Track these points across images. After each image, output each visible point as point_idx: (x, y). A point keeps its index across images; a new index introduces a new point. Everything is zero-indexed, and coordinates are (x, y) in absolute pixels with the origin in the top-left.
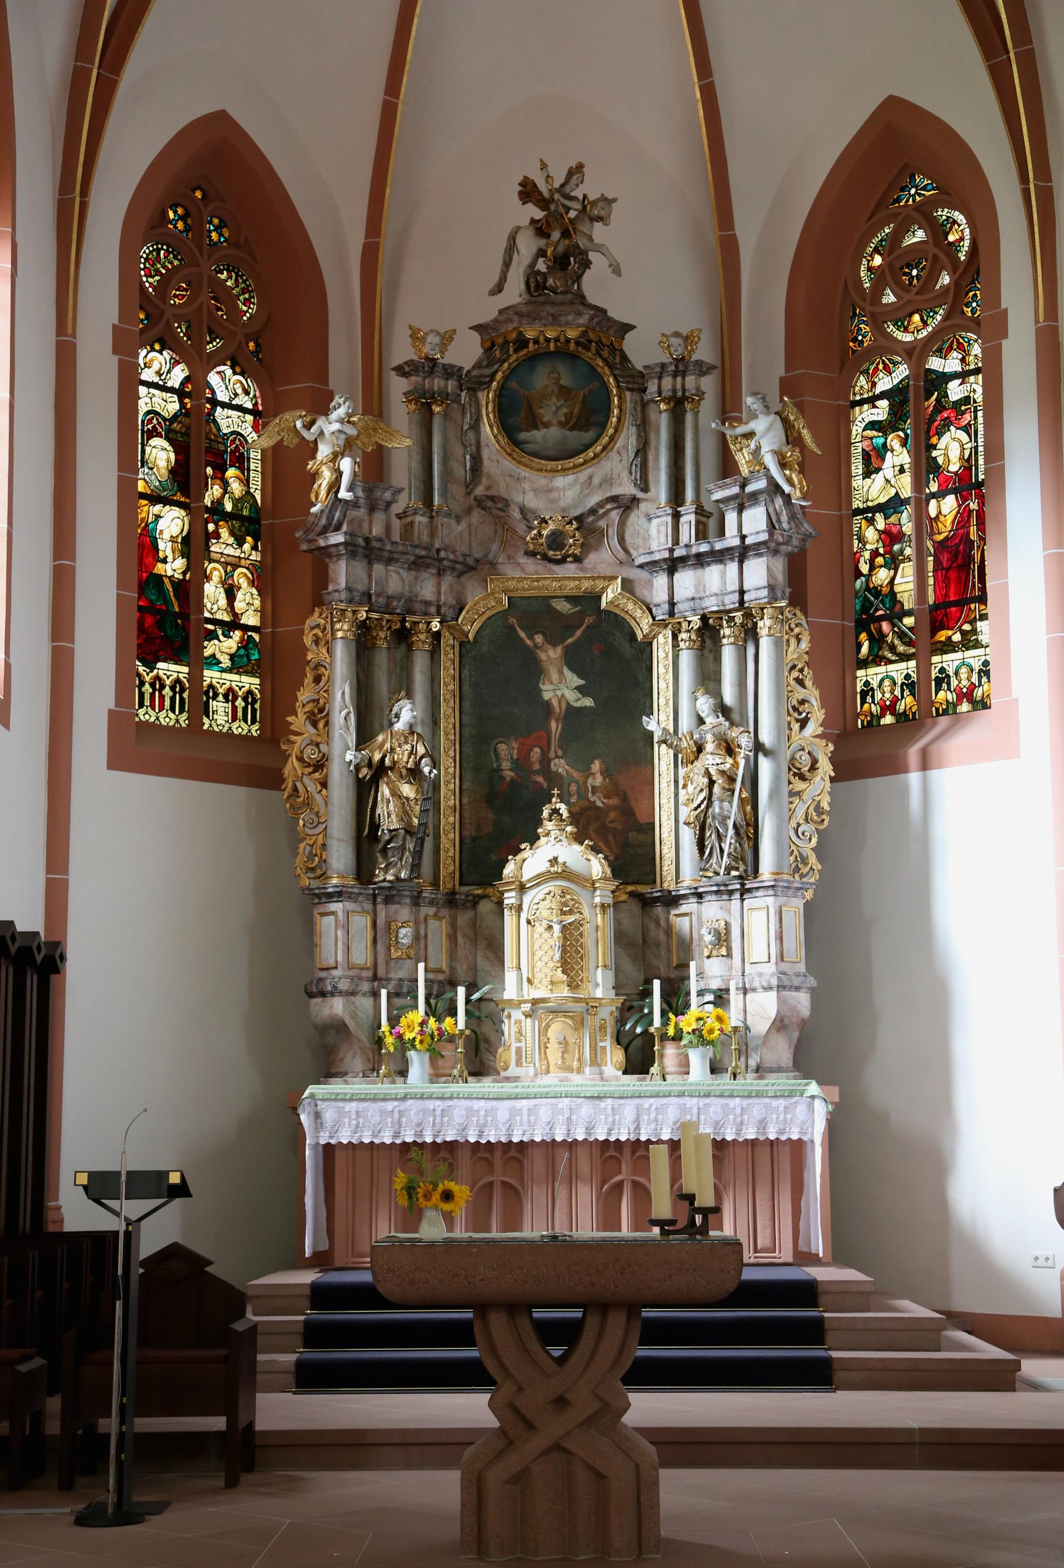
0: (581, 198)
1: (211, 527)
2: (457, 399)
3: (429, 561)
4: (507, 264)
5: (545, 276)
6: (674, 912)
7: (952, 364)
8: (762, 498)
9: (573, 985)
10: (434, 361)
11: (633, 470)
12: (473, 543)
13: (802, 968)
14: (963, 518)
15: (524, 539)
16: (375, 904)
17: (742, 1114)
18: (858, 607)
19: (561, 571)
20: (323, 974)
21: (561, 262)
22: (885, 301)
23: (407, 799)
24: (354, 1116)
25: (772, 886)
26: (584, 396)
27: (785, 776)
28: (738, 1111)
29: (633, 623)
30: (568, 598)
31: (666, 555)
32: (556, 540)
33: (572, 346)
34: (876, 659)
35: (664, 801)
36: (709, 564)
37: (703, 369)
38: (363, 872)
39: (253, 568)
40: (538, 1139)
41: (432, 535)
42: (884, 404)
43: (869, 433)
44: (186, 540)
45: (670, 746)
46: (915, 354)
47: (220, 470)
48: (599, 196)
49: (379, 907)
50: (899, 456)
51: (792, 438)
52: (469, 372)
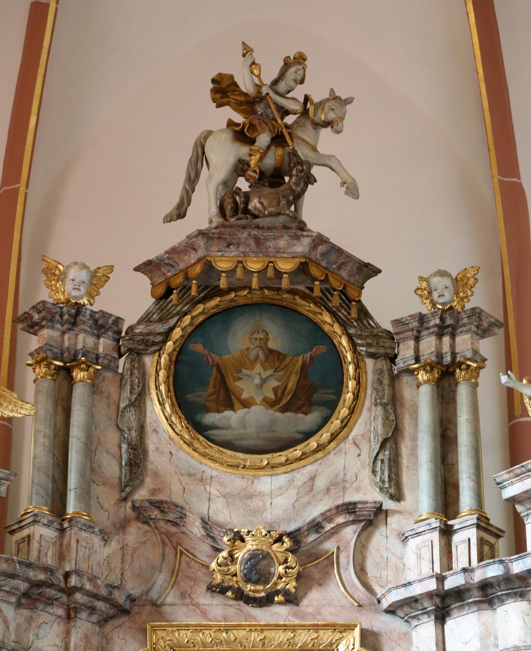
0: (302, 100)
2: (111, 367)
3: (51, 592)
5: (247, 197)
10: (79, 308)
11: (378, 469)
12: (128, 575)
15: (208, 567)
26: (304, 365)
31: (432, 585)
33: (285, 283)
36: (502, 602)
41: (61, 557)
48: (327, 96)
52: (131, 328)
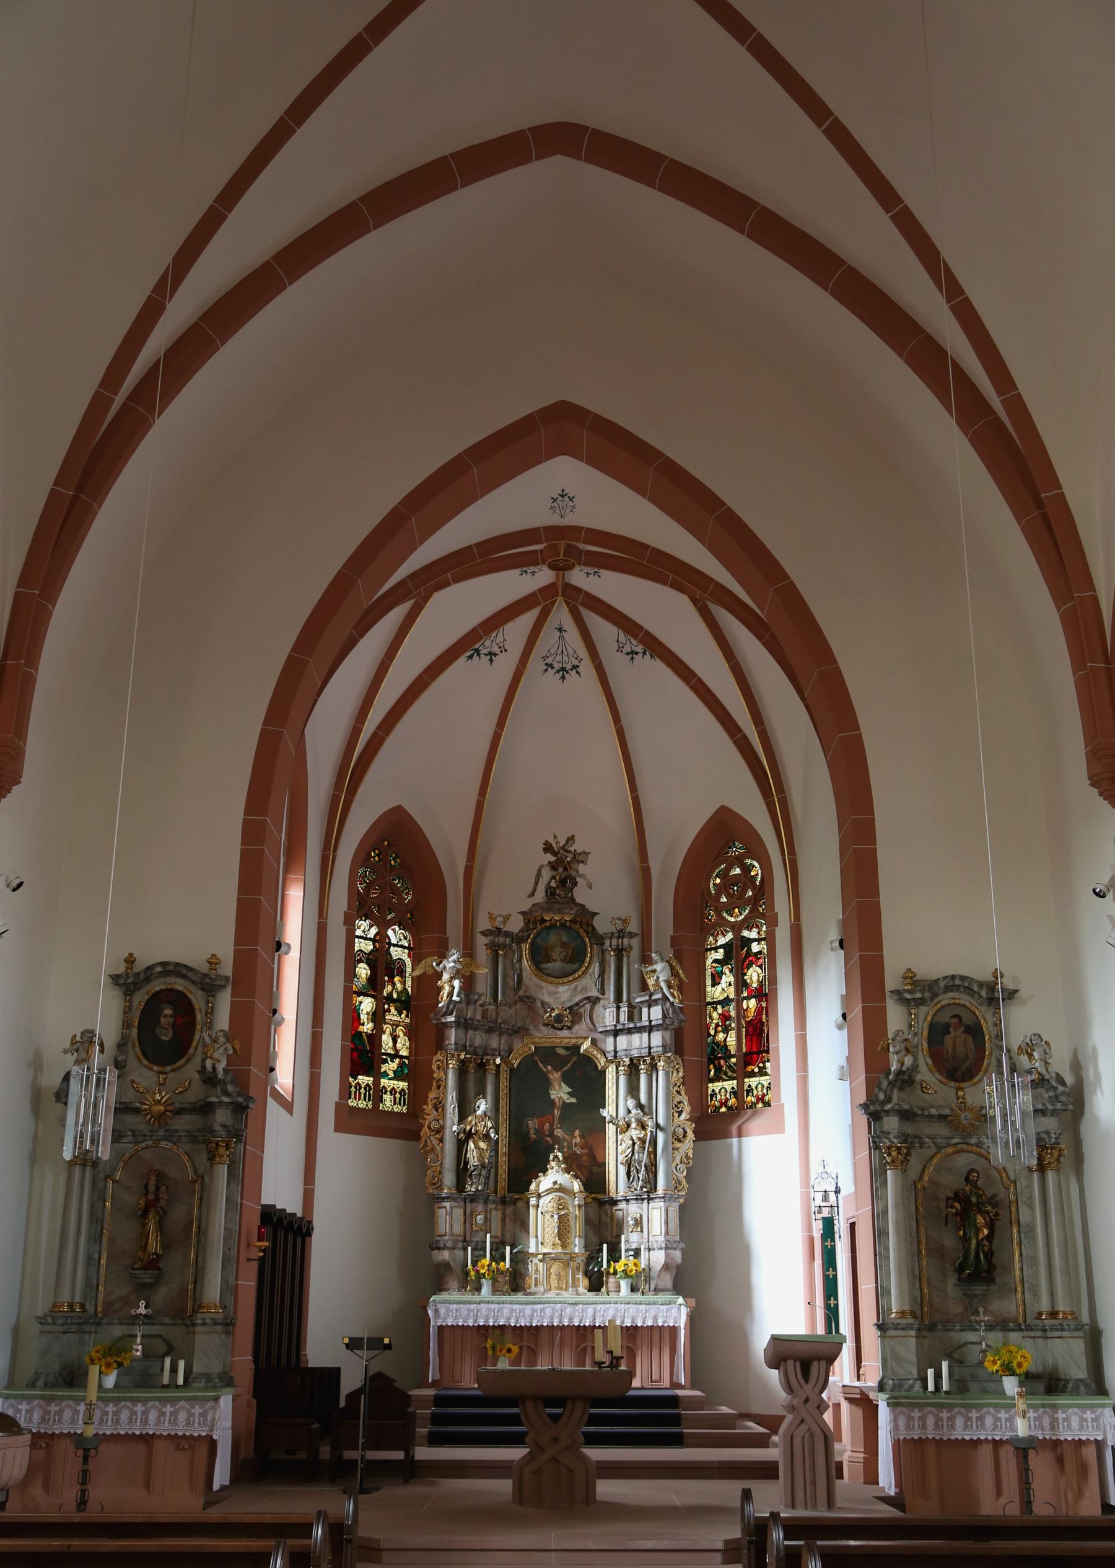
1: (386, 1006)
3: (495, 1029)
4: (537, 883)
5: (555, 889)
6: (615, 1208)
7: (753, 934)
8: (660, 1002)
9: (564, 1246)
13: (677, 1238)
14: (759, 1010)
16: (465, 1203)
17: (645, 1313)
18: (709, 1051)
19: (562, 1034)
20: (439, 1238)
21: (563, 882)
22: (721, 901)
23: (483, 1149)
24: (454, 1311)
25: (663, 1197)
27: (671, 1140)
28: (644, 1311)
29: (596, 1061)
30: (565, 1048)
31: (613, 1028)
32: (559, 1019)
34: (717, 1079)
35: (611, 1151)
36: (634, 1033)
37: (632, 935)
38: (460, 1186)
39: (406, 1026)
40: (545, 1324)
41: (497, 1015)
42: (721, 951)
43: (714, 965)
44: (374, 1014)
45: (614, 1124)
46: (736, 928)
47: (391, 978)
49: (467, 1204)
50: (728, 978)
51: (674, 973)
52: (517, 934)
